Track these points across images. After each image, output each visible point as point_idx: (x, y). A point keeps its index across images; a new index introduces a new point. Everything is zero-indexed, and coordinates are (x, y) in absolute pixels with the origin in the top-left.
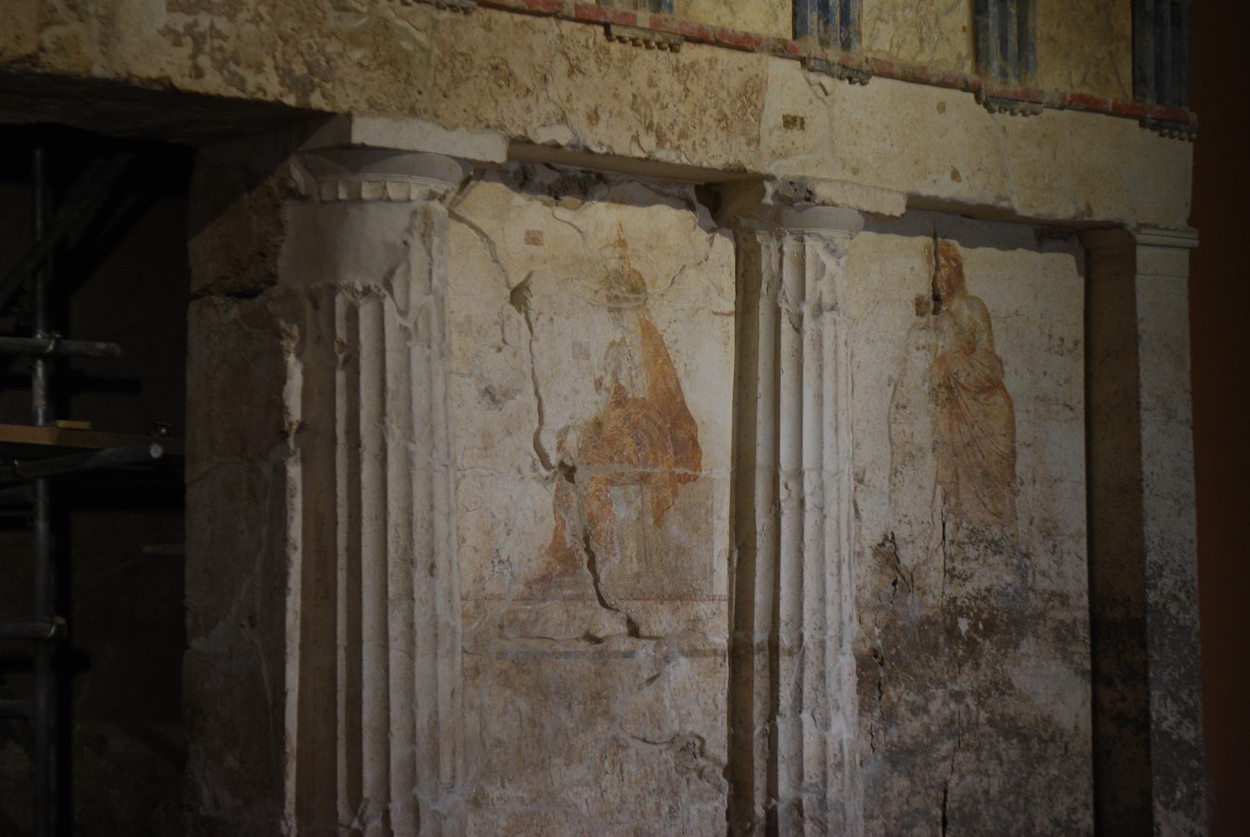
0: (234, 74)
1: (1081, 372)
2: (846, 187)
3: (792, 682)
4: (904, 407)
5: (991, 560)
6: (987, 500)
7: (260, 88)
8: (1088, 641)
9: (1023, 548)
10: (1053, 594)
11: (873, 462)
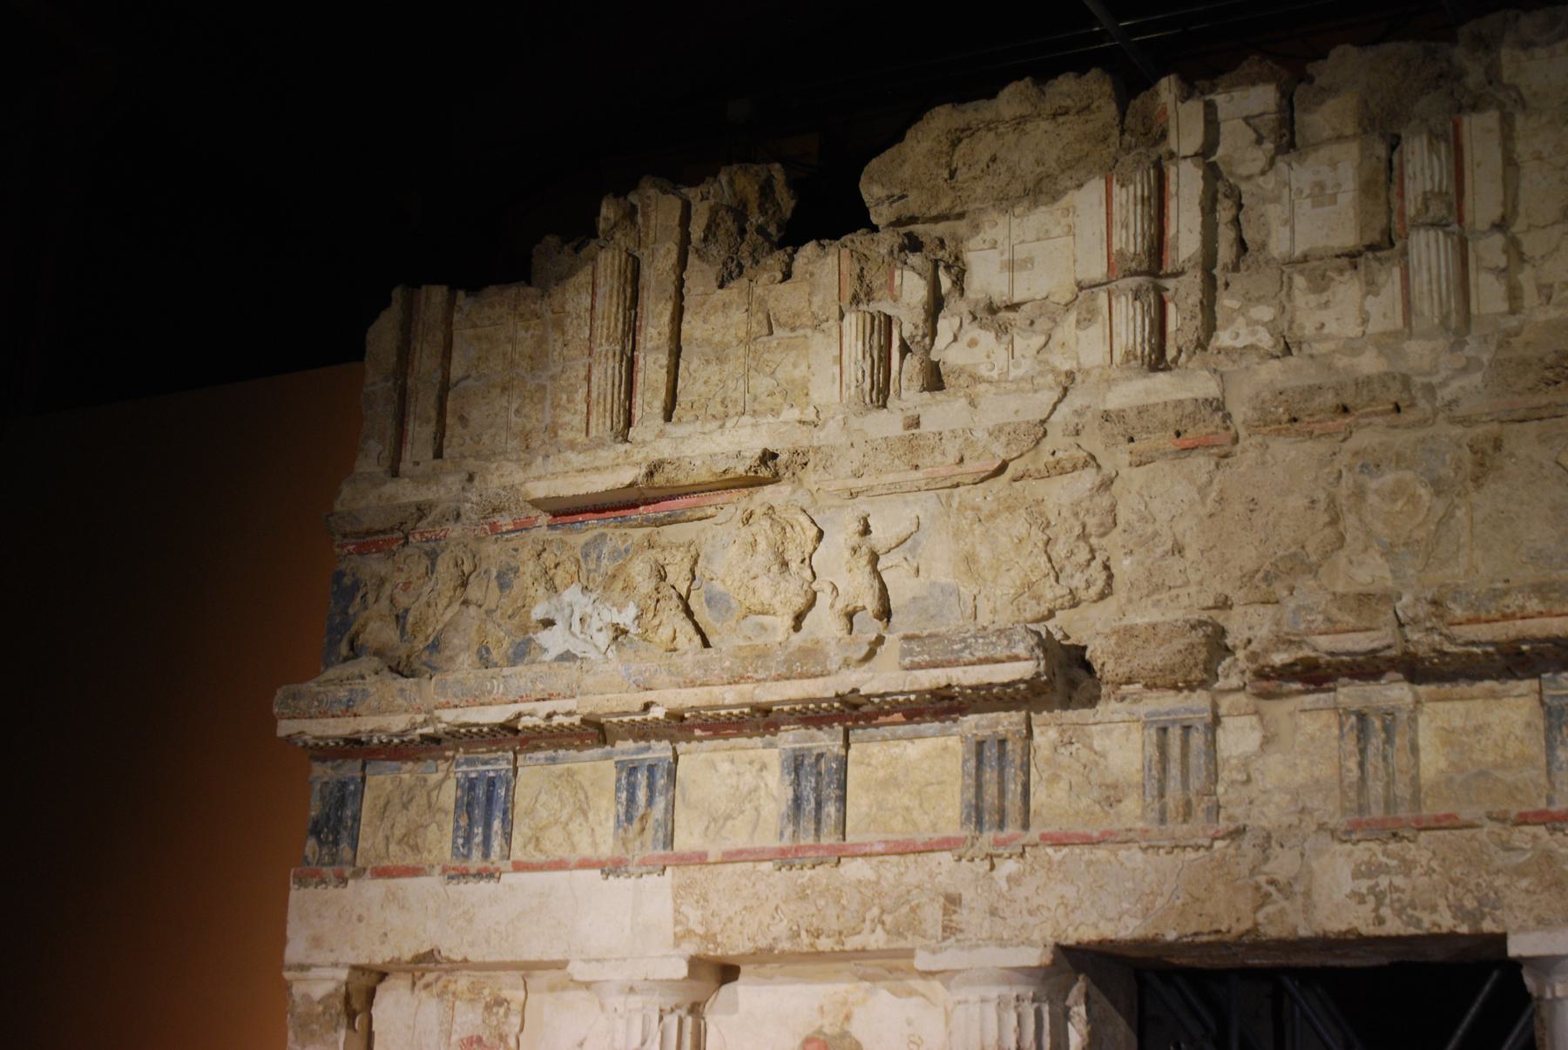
0: (1411, 917)
7: (1434, 924)
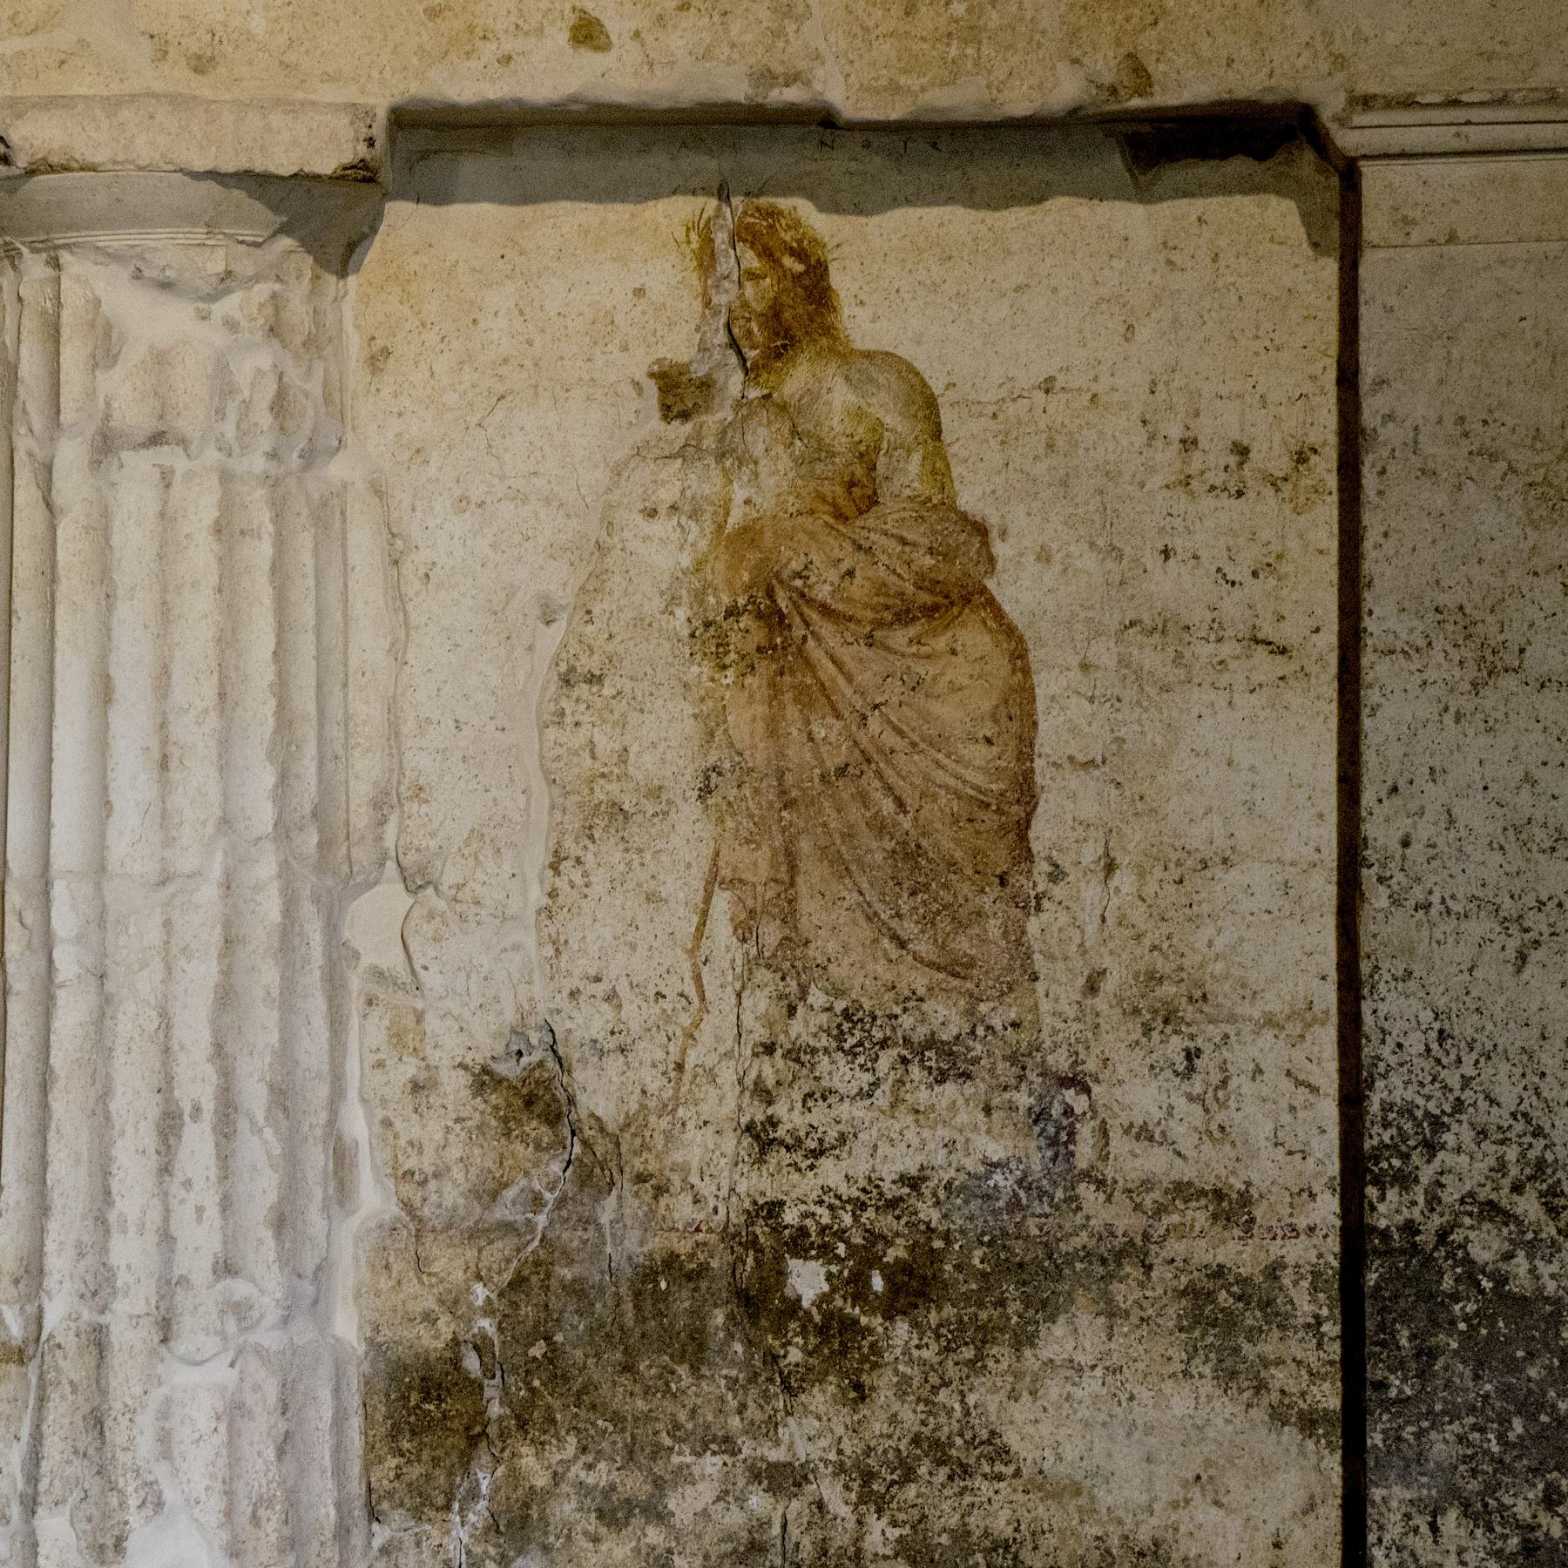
1: (1327, 537)
2: (125, 114)
3: (25, 1433)
4: (594, 679)
5: (923, 1096)
6: (908, 928)
8: (1331, 1329)
9: (1060, 1061)
10: (1182, 1191)
11: (476, 834)
